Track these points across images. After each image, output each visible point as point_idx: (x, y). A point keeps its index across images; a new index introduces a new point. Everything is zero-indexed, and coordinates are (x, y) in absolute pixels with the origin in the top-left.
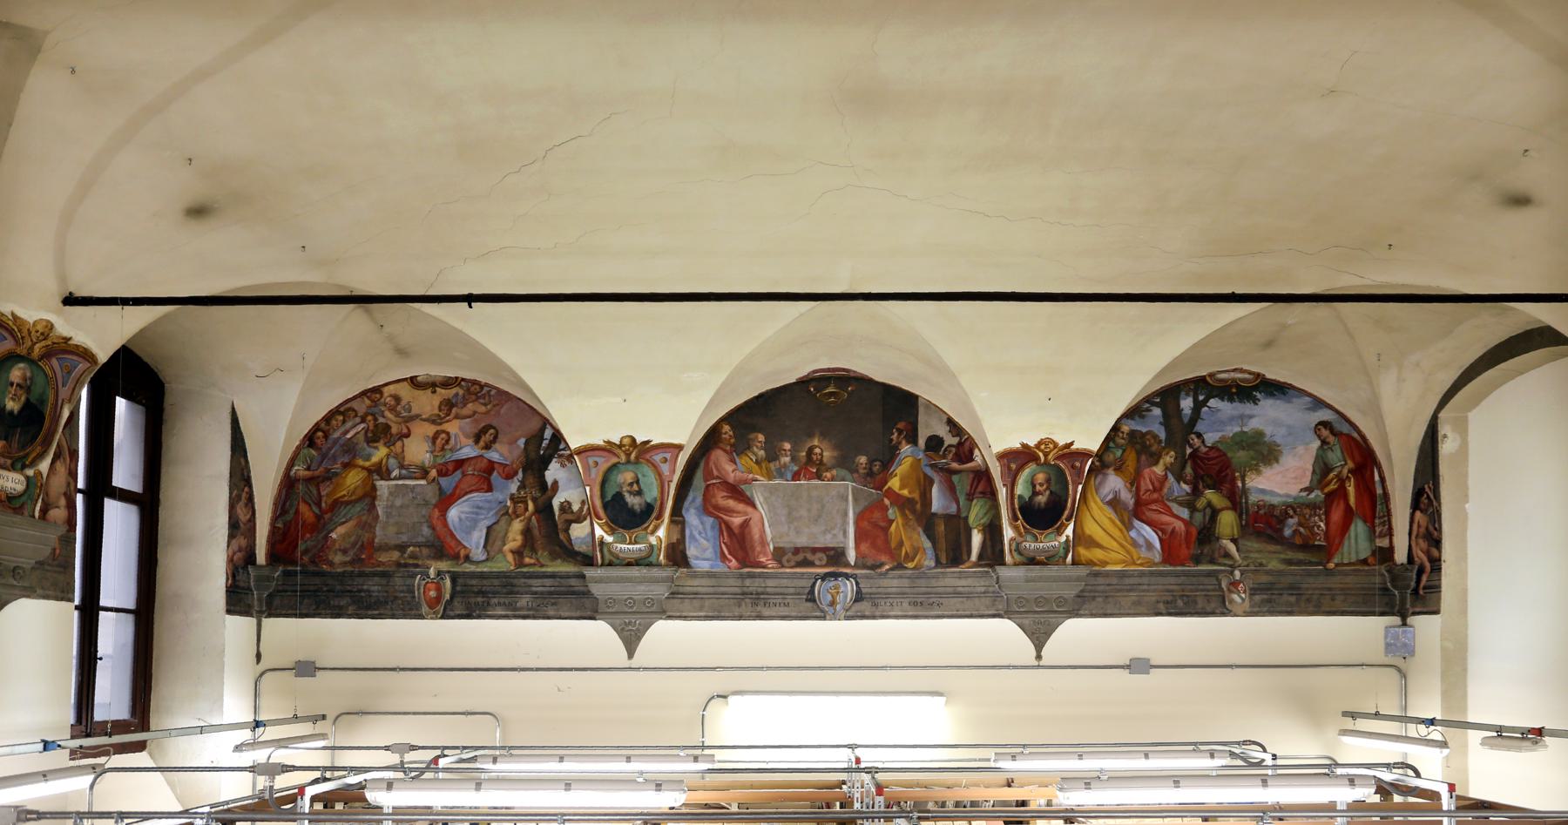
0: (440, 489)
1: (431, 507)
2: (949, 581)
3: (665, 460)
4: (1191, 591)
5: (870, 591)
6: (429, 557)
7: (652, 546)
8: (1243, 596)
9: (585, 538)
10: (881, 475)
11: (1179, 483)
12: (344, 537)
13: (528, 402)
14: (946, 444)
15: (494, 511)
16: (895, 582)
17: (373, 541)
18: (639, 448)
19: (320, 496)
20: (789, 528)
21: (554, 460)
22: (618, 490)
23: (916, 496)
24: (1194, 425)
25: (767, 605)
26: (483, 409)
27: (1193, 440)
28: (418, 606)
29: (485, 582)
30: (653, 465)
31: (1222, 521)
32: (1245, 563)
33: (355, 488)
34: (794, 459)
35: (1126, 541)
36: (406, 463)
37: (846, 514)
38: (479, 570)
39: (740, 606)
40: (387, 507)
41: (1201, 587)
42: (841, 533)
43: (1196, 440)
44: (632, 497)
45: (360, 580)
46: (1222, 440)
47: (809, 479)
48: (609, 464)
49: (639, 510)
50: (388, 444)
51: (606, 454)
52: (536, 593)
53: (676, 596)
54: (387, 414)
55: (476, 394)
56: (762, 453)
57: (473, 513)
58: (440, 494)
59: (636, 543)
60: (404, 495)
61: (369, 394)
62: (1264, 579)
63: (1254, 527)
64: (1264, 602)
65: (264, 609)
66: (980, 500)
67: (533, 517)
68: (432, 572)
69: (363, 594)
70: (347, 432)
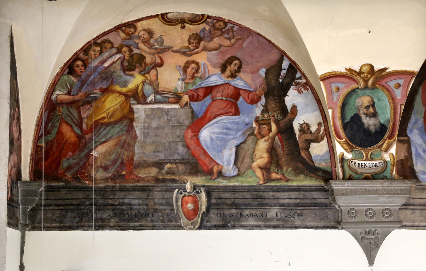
0: (192, 112)
1: (185, 128)
3: (399, 86)
6: (185, 173)
7: (386, 162)
9: (323, 156)
12: (105, 155)
13: (267, 37)
15: (241, 132)
17: (133, 159)
18: (376, 74)
19: (81, 119)
21: (292, 87)
26: (227, 43)
28: (177, 218)
29: (237, 195)
30: (388, 90)
33: (114, 111)
36: (160, 89)
38: (231, 184)
40: (144, 128)
44: (368, 118)
45: (122, 194)
48: (349, 90)
49: (374, 130)
50: (143, 73)
51: (346, 80)
52: (283, 205)
54: (141, 45)
55: (221, 30)
57: (222, 133)
58: (193, 117)
59: (372, 159)
60: (159, 118)
61: (124, 28)
65: (28, 222)
67: (277, 137)
68: (188, 187)
69: (124, 207)
70: (104, 61)
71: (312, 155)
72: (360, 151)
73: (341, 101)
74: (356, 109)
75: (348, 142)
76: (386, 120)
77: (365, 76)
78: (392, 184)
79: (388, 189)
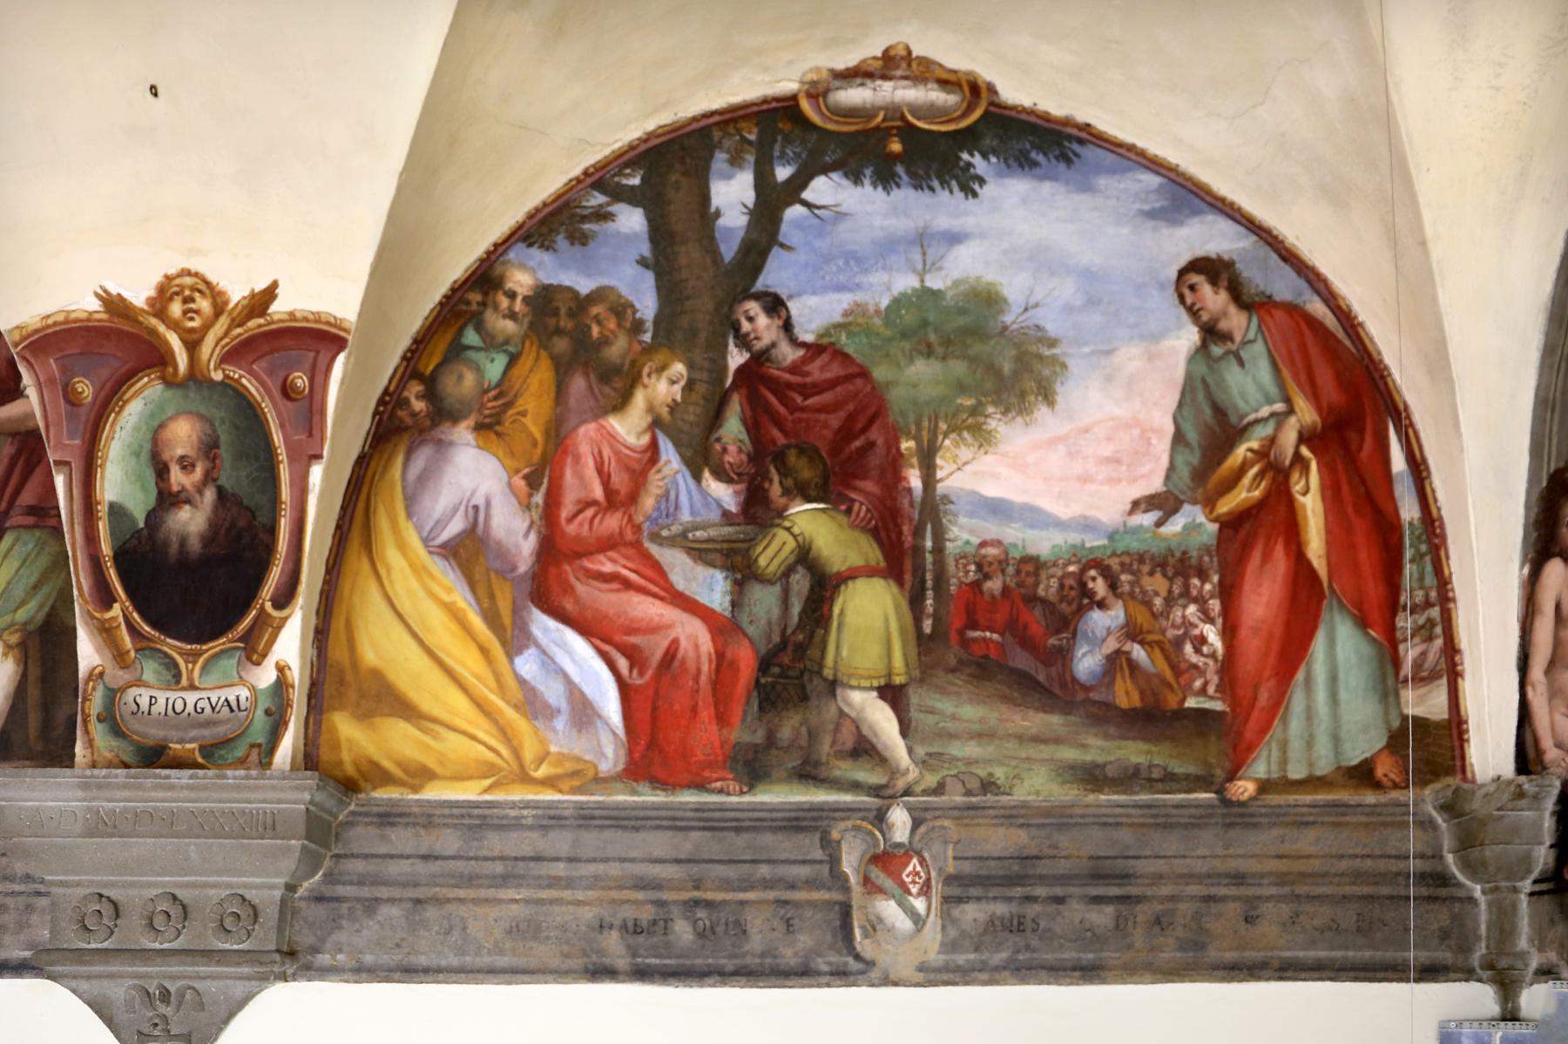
4: (726, 885)
8: (919, 904)
11: (697, 477)
24: (757, 270)
27: (751, 319)
31: (850, 618)
32: (931, 780)
35: (501, 688)
41: (764, 870)
43: (762, 320)
46: (853, 322)
62: (999, 840)
63: (965, 643)
64: (992, 926)
66: (25, 535)
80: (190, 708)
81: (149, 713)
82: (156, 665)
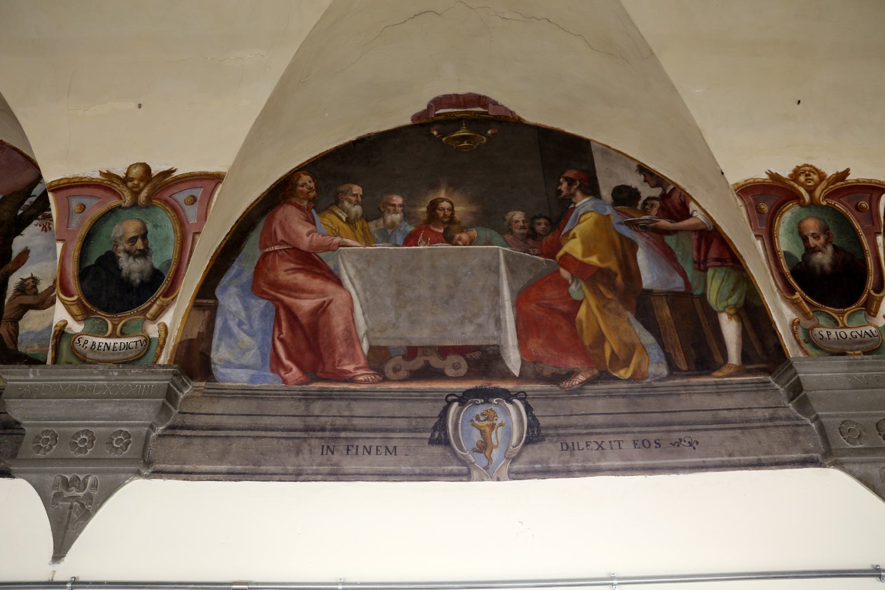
2: (698, 401)
5: (554, 421)
7: (148, 341)
10: (550, 237)
14: (644, 196)
16: (600, 405)
18: (155, 181)
20: (398, 316)
21: (35, 222)
22: (109, 248)
23: (612, 264)
25: (353, 451)
30: (174, 209)
34: (407, 217)
37: (497, 292)
39: (298, 452)
42: (492, 322)
44: (131, 260)
47: (432, 243)
48: (103, 209)
49: (138, 281)
53: (179, 432)
56: (357, 209)
59: (123, 334)
66: (719, 269)
71: (20, 332)
72: (104, 320)
73: (86, 228)
74: (111, 242)
75: (82, 303)
76: (163, 263)
77: (134, 184)
78: (126, 374)
79: (121, 386)
80: (849, 336)
81: (829, 339)
82: (824, 318)
